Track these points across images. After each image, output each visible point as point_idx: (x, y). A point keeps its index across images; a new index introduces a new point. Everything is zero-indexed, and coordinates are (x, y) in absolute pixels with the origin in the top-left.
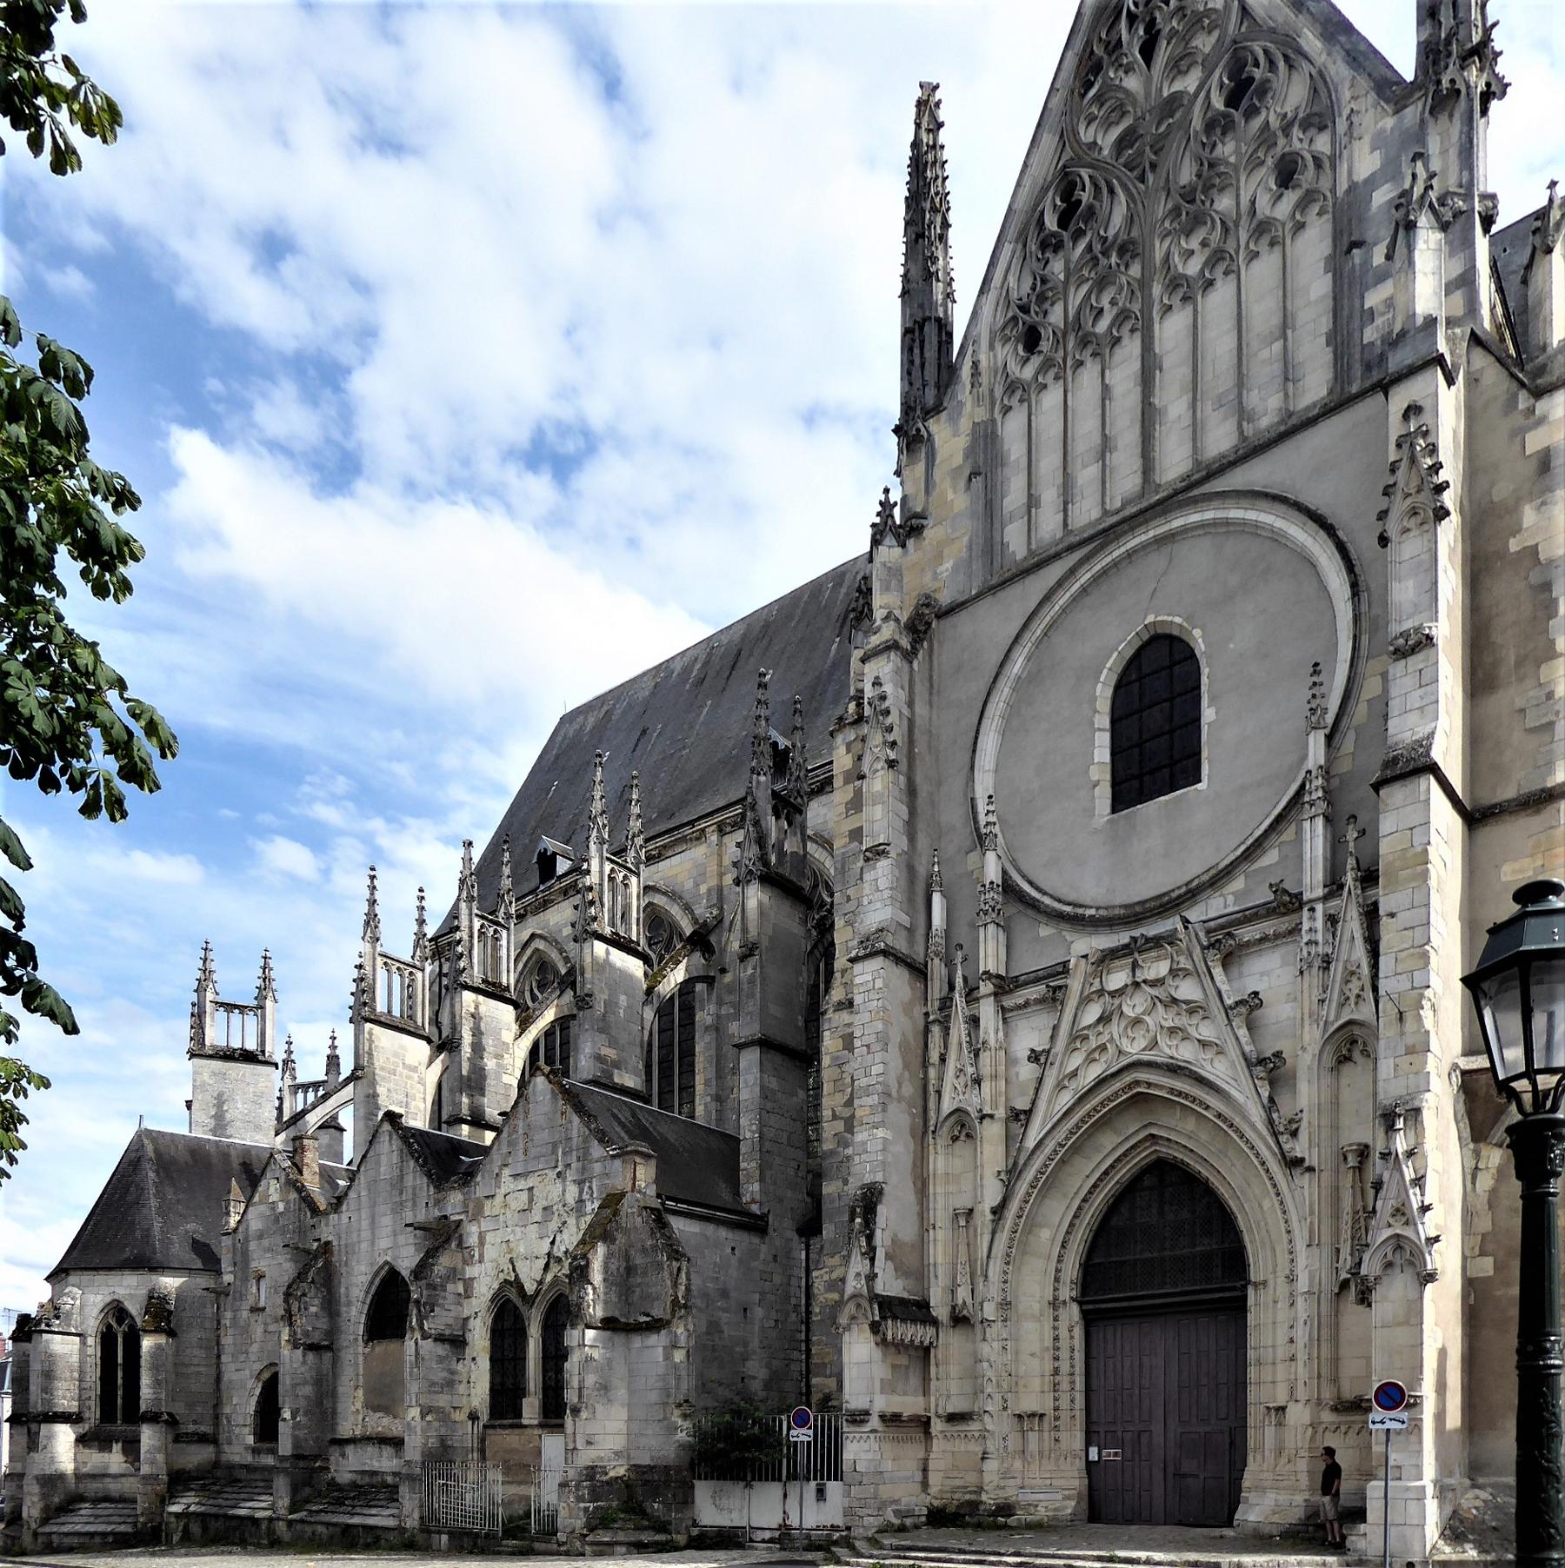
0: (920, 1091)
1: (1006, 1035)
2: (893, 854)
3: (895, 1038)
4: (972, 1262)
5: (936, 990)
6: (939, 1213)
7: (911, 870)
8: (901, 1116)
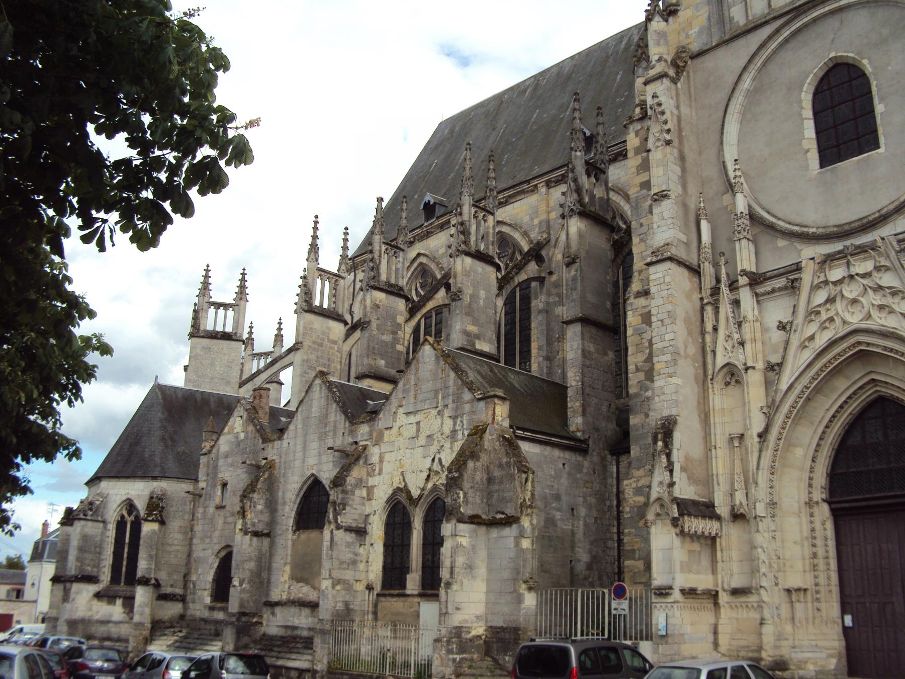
0: (700, 351)
1: (760, 312)
2: (673, 196)
3: (680, 314)
4: (745, 472)
5: (708, 282)
6: (718, 437)
7: (685, 206)
8: (687, 369)
